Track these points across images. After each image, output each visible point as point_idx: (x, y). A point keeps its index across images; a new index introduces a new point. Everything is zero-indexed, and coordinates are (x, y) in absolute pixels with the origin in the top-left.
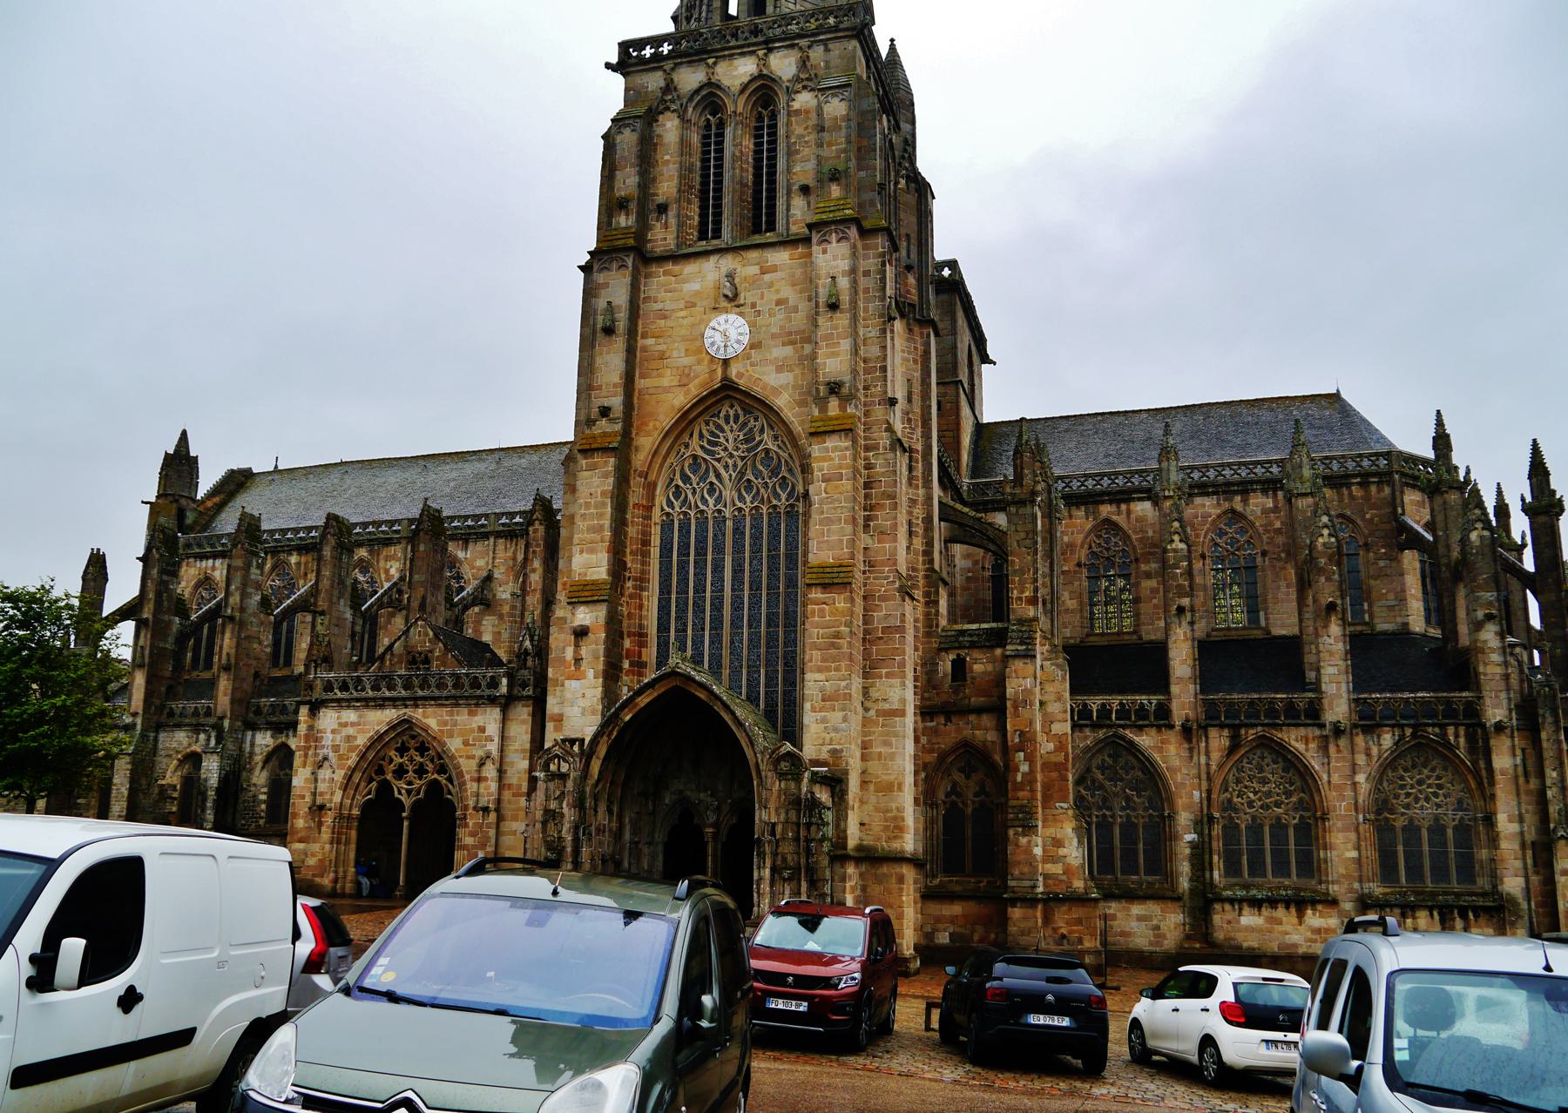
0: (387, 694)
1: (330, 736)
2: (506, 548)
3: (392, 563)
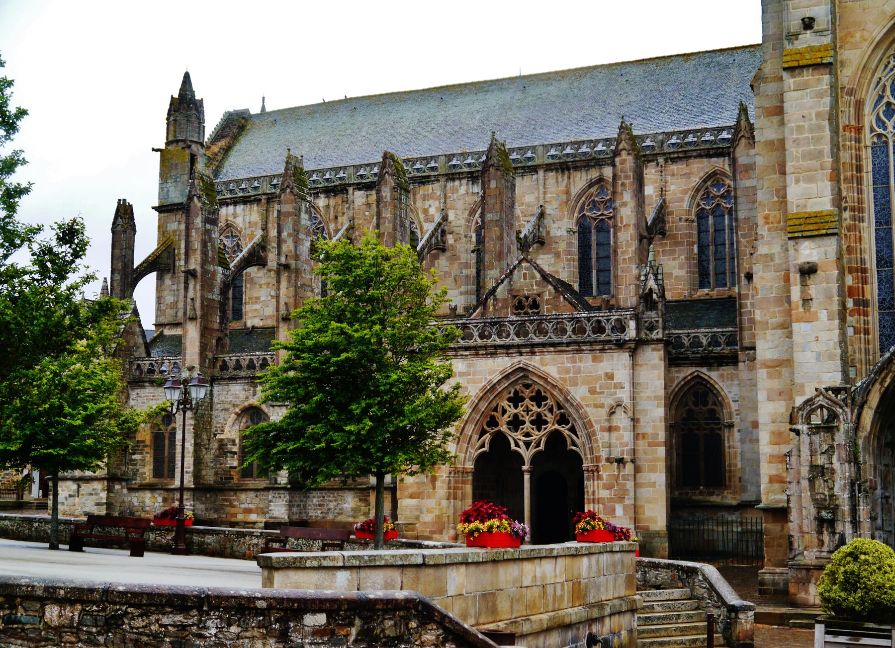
0: (499, 342)
2: (557, 182)
3: (431, 202)
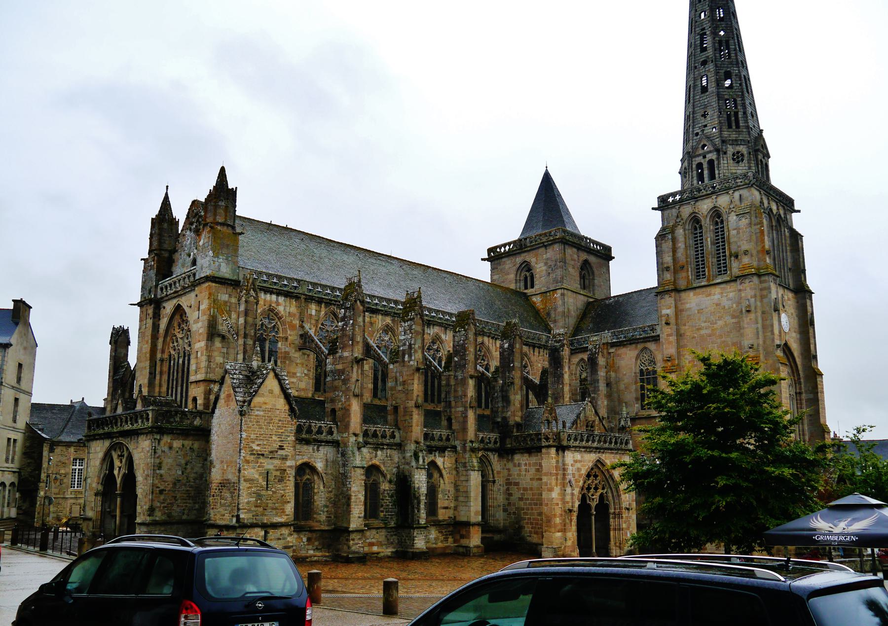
1: (571, 467)
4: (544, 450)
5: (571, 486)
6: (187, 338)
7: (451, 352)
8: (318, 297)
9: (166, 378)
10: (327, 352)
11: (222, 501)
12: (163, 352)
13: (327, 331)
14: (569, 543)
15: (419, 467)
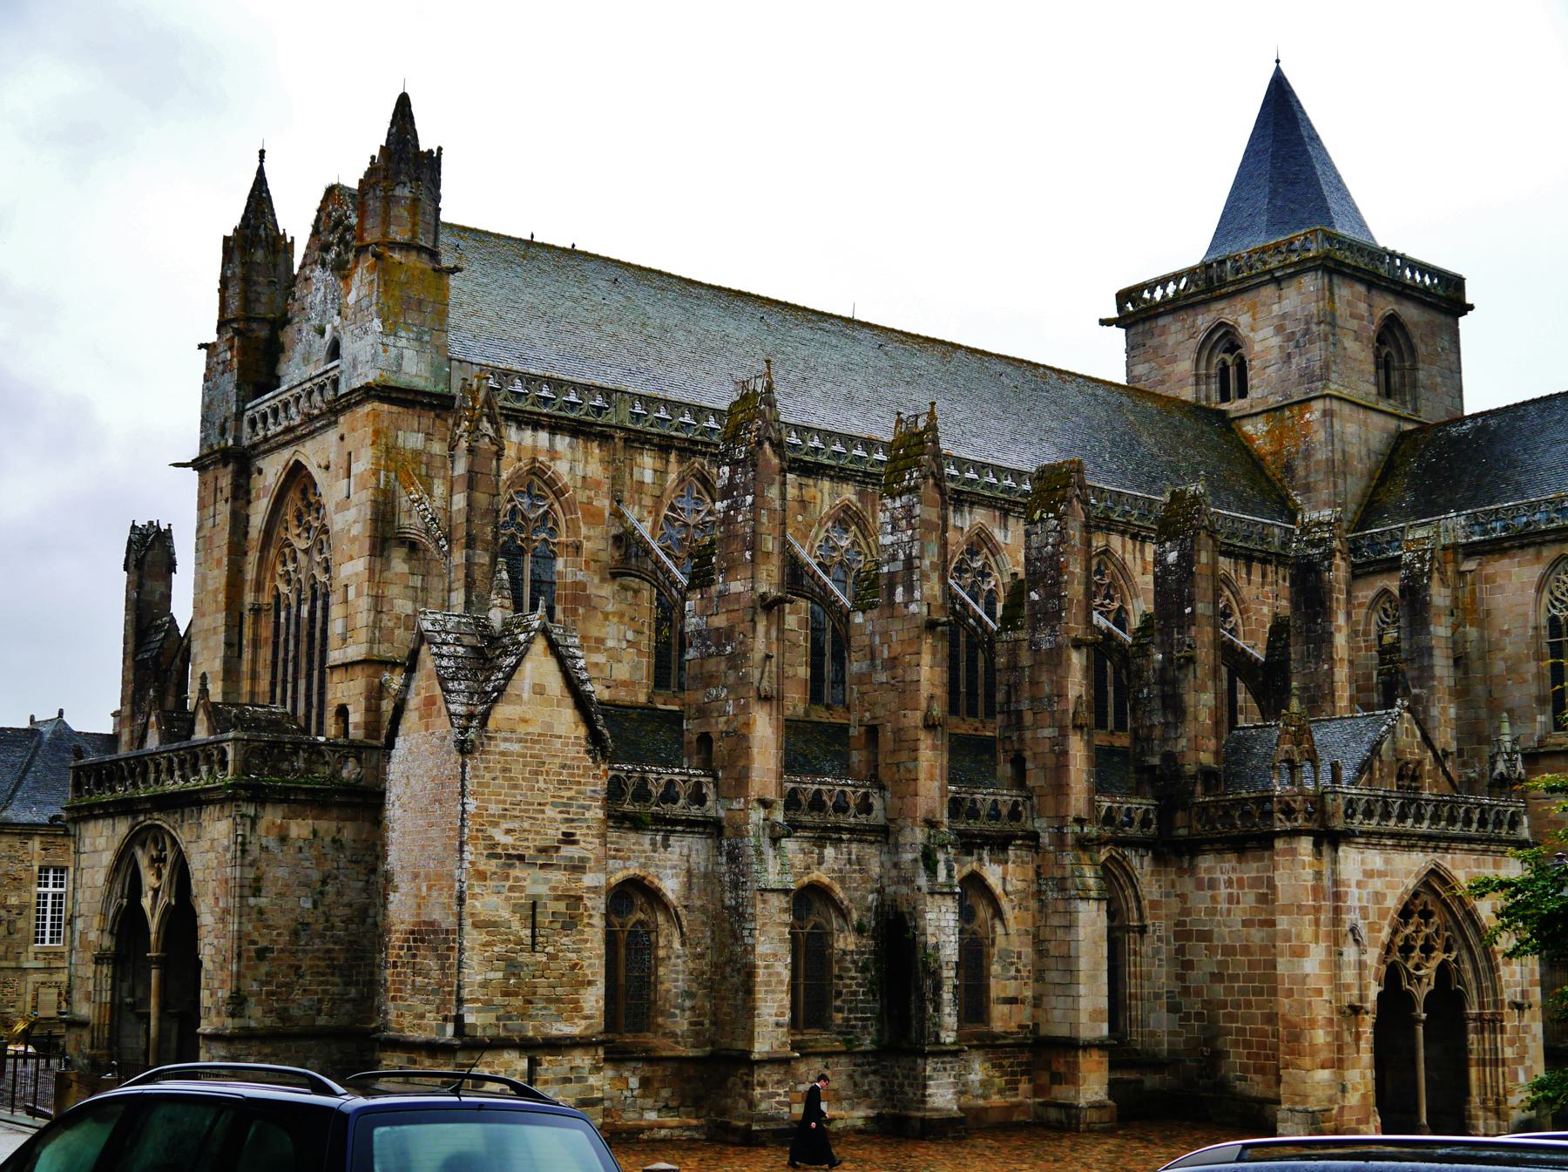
4: (1279, 844)
5: (1356, 941)
6: (321, 552)
7: (1022, 575)
8: (659, 435)
9: (269, 657)
10: (685, 582)
11: (418, 979)
12: (259, 587)
13: (686, 525)
14: (1353, 1099)
15: (937, 889)
